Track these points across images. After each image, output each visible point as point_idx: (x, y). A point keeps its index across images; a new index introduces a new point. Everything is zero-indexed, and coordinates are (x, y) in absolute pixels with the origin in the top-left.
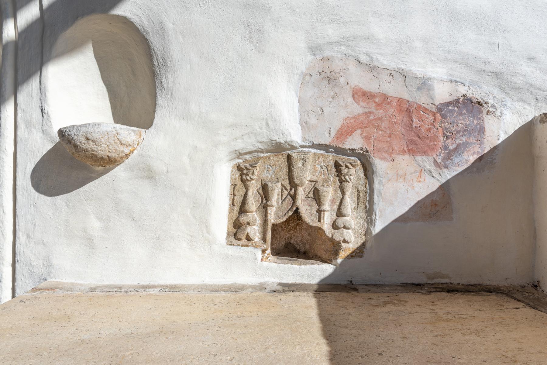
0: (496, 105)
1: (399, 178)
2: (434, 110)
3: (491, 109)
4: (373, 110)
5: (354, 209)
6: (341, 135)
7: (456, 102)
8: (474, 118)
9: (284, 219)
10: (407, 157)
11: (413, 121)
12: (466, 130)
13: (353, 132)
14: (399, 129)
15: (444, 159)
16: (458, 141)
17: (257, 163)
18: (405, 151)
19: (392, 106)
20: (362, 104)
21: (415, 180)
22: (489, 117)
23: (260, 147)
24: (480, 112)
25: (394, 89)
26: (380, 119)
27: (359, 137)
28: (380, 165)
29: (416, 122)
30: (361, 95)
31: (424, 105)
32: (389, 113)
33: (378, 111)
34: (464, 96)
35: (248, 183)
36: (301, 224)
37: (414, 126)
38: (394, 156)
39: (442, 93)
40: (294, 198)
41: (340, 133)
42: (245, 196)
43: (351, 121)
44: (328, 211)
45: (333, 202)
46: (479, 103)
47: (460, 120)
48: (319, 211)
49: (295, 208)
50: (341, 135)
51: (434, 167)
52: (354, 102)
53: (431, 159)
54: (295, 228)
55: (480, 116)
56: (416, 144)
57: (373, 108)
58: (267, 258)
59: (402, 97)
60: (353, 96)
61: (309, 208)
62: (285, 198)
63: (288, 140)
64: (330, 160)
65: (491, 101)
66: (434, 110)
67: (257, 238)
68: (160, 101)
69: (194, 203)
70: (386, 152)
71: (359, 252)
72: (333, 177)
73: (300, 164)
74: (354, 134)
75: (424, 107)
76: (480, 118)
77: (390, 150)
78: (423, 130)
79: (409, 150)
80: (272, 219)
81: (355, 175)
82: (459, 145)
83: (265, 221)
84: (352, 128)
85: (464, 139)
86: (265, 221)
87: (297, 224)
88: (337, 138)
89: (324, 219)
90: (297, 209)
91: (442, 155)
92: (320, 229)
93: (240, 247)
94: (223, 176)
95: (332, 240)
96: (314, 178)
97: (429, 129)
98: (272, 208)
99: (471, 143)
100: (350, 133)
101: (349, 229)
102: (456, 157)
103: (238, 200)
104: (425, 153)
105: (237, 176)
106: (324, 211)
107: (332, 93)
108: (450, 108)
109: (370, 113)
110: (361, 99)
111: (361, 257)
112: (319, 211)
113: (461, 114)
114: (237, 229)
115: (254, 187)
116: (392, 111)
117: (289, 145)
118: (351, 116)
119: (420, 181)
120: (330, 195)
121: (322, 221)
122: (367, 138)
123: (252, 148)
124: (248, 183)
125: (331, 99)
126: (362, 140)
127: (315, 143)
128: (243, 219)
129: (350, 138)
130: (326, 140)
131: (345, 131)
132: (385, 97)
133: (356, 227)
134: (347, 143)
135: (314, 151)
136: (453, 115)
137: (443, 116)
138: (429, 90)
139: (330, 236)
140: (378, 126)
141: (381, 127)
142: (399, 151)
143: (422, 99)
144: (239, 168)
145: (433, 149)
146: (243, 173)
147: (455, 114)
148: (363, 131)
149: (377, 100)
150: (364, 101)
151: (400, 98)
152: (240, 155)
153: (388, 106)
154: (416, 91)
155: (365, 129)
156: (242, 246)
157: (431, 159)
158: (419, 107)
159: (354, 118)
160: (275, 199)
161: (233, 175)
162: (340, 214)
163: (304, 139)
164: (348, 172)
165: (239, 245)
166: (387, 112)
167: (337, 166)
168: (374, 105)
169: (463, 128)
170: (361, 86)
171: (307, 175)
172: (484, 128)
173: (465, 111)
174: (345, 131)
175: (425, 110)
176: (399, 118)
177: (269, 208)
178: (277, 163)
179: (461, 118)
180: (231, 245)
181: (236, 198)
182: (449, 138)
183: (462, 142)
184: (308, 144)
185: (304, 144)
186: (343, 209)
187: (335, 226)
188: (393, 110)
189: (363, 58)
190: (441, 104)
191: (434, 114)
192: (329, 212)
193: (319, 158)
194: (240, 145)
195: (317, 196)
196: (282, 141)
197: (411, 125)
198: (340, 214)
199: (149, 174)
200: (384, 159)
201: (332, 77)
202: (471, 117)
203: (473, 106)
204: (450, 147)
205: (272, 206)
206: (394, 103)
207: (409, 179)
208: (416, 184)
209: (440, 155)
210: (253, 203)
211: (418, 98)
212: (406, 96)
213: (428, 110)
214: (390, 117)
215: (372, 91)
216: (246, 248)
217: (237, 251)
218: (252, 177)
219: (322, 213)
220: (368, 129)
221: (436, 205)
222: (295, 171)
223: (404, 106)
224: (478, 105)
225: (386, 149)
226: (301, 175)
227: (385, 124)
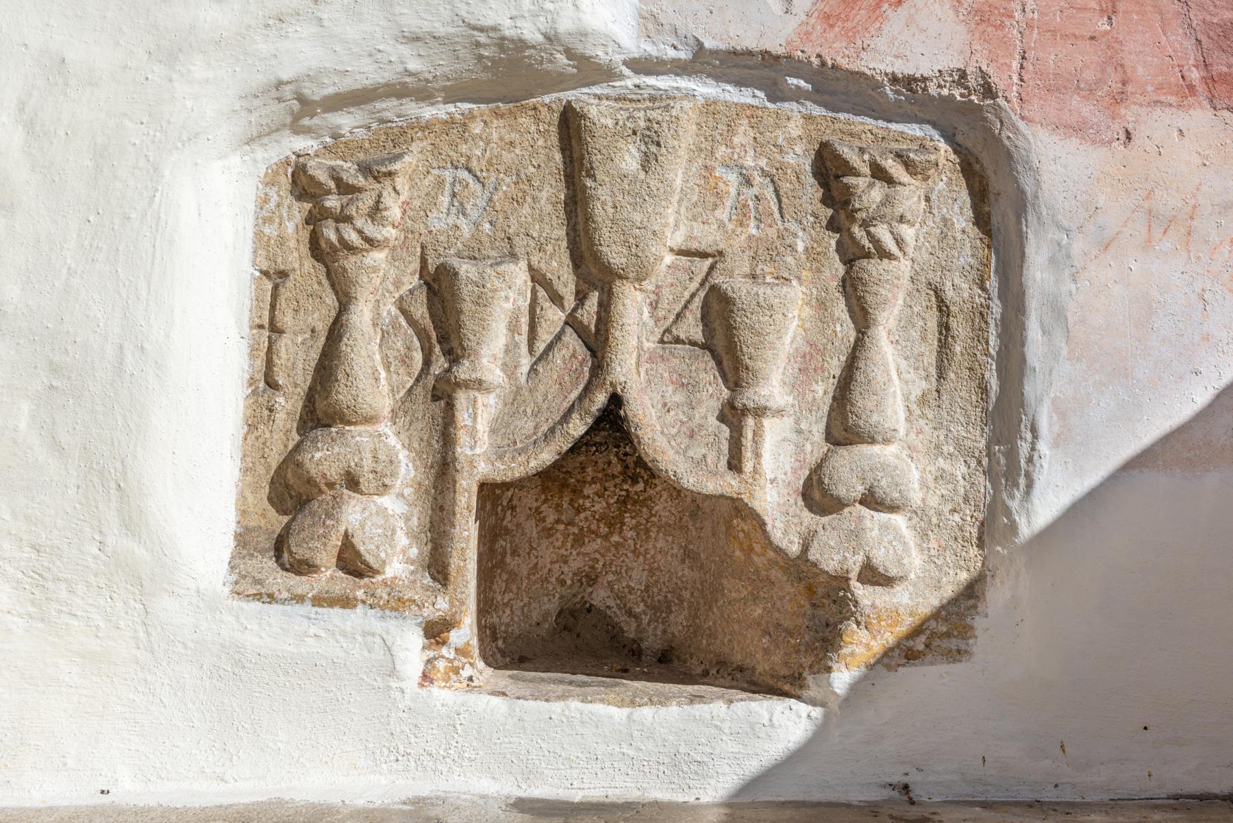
1: (1157, 233)
5: (923, 400)
9: (547, 456)
17: (398, 157)
18: (1191, 87)
23: (413, 65)
28: (1057, 163)
35: (350, 263)
36: (647, 502)
38: (1129, 114)
40: (597, 342)
42: (336, 331)
44: (780, 412)
45: (807, 365)
48: (733, 415)
49: (601, 399)
54: (615, 523)
58: (456, 671)
61: (679, 398)
62: (550, 347)
63: (565, 25)
64: (791, 141)
67: (398, 560)
69: (54, 369)
71: (943, 633)
72: (806, 234)
73: (630, 160)
79: (1210, 80)
80: (481, 454)
81: (923, 218)
83: (443, 469)
86: (443, 469)
87: (623, 502)
88: (828, 19)
89: (758, 455)
90: (616, 400)
92: (739, 510)
93: (307, 608)
94: (214, 225)
95: (801, 569)
96: (708, 237)
98: (481, 399)
101: (893, 508)
103: (297, 358)
106: (760, 412)
111: (957, 655)
112: (733, 415)
114: (292, 515)
115: (383, 286)
117: (569, 53)
120: (789, 324)
121: (748, 466)
123: (368, 74)
124: (350, 263)
126: (962, 28)
127: (709, 44)
129: (895, 21)
133: (933, 501)
134: (880, 43)
135: (705, 89)
139: (795, 549)
142: (1159, 88)
144: (303, 185)
146: (320, 212)
152: (303, 108)
156: (318, 601)
160: (494, 350)
162: (844, 427)
163: (650, 22)
164: (887, 201)
165: (300, 599)
167: (829, 170)
171: (668, 220)
177: (461, 398)
178: (507, 157)
180: (258, 597)
181: (285, 346)
184: (672, 53)
185: (651, 50)
186: (862, 401)
192: (788, 422)
194: (304, 55)
195: (720, 333)
196: (531, 32)
198: (844, 427)
200: (1078, 129)
205: (479, 385)
216: (337, 610)
218: (371, 230)
219: (750, 422)
222: (604, 199)
225: (1089, 75)
226: (637, 217)
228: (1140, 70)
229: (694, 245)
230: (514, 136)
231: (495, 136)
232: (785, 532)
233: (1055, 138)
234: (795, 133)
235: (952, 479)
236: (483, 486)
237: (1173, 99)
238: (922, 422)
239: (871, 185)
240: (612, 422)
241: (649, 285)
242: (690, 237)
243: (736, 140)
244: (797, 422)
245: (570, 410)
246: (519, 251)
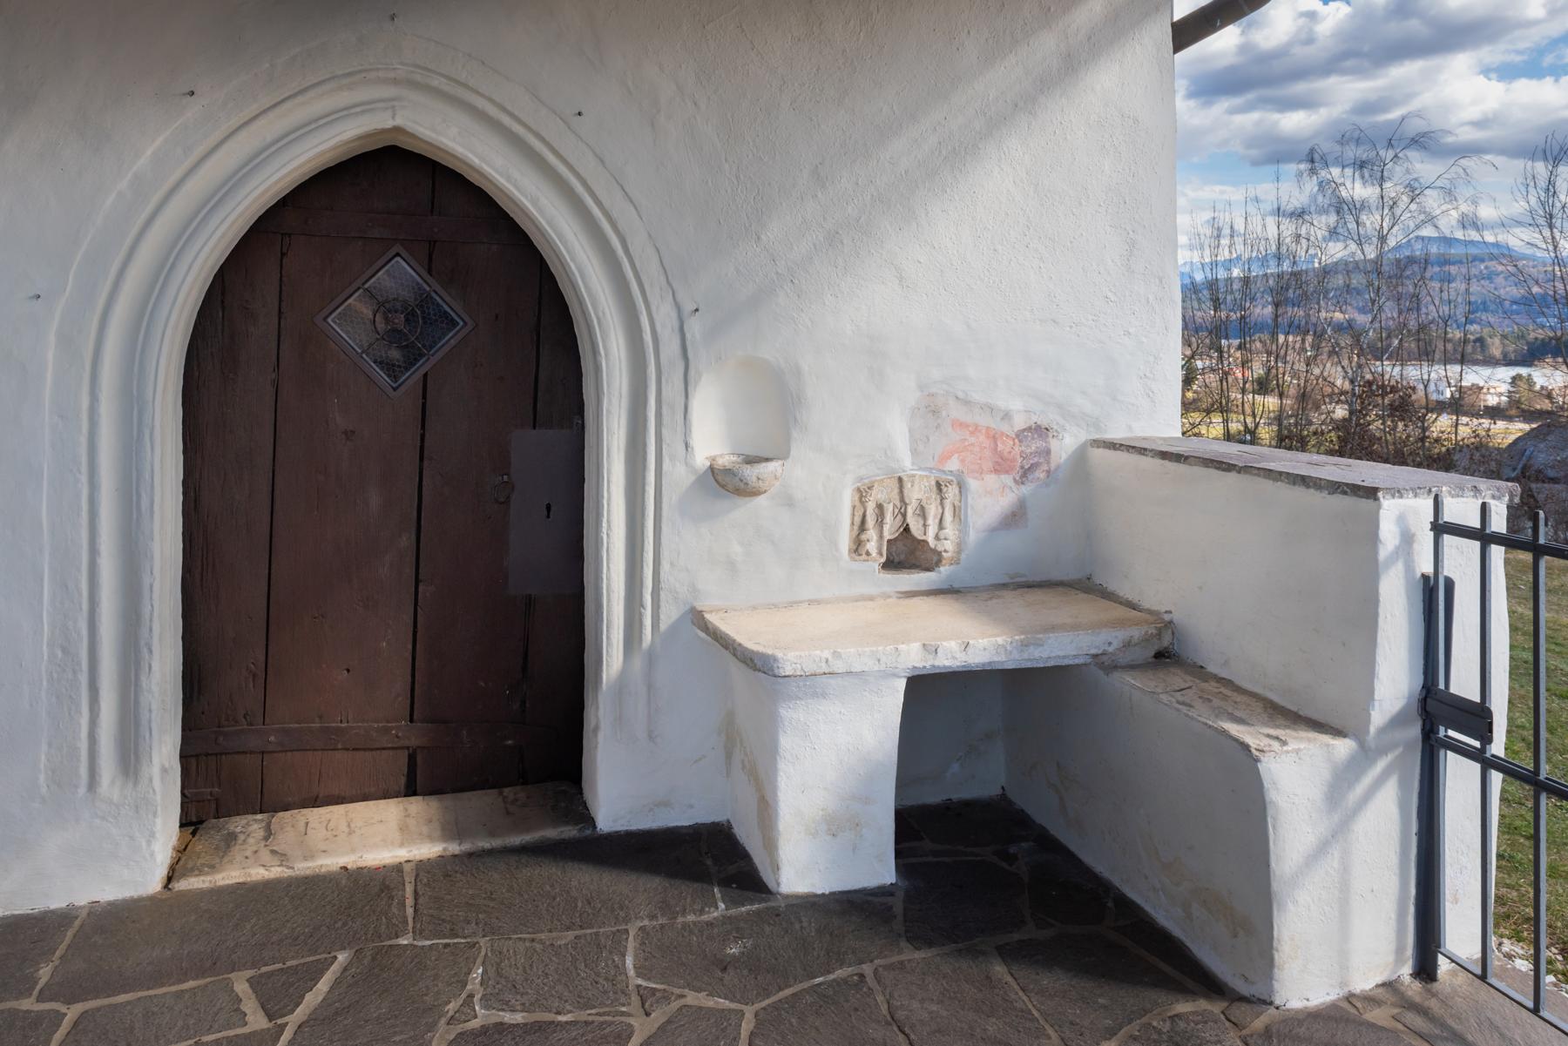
7: (1029, 429)
10: (993, 476)
14: (988, 453)
25: (984, 420)
28: (973, 484)
29: (1000, 447)
39: (1020, 422)
40: (904, 516)
42: (864, 516)
48: (925, 525)
67: (874, 553)
68: (795, 434)
71: (956, 561)
72: (934, 495)
80: (887, 536)
81: (951, 492)
83: (881, 537)
86: (881, 537)
92: (925, 541)
94: (847, 498)
103: (858, 520)
104: (1007, 472)
112: (925, 525)
114: (858, 546)
115: (871, 506)
116: (982, 438)
120: (933, 511)
122: (963, 461)
128: (863, 537)
130: (931, 464)
143: (1005, 428)
144: (859, 490)
146: (862, 494)
160: (889, 518)
162: (941, 526)
167: (938, 485)
171: (914, 494)
187: (937, 538)
189: (961, 395)
195: (922, 513)
198: (941, 526)
199: (789, 502)
210: (871, 522)
212: (993, 425)
217: (859, 566)
222: (906, 492)
227: (977, 449)
240: (907, 529)
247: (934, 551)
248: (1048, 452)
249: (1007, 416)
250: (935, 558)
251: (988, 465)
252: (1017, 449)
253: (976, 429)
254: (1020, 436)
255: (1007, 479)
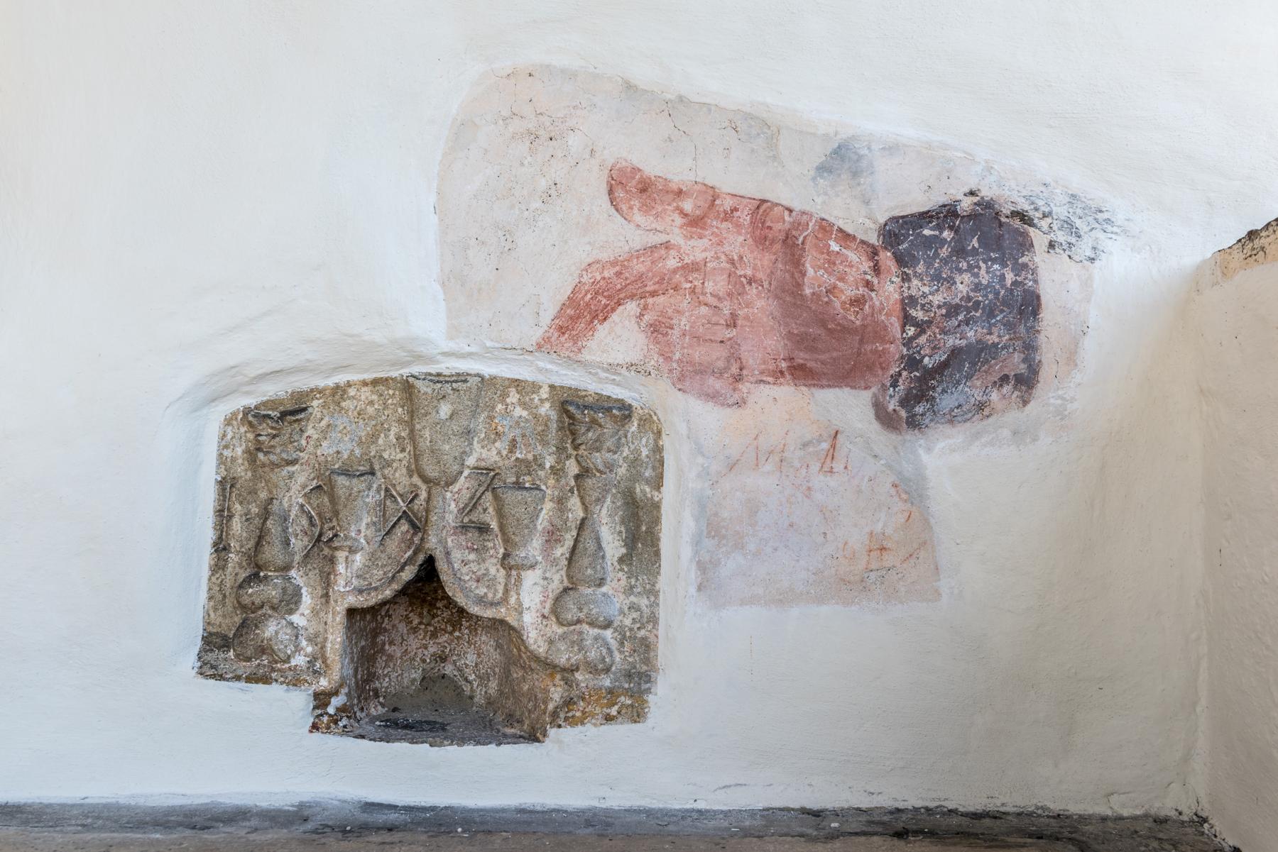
0: (1078, 223)
2: (873, 239)
3: (1061, 237)
4: (677, 238)
5: (621, 560)
6: (574, 319)
7: (947, 214)
8: (1004, 265)
11: (804, 274)
12: (977, 303)
13: (613, 310)
14: (760, 305)
15: (905, 402)
16: (952, 341)
17: (304, 409)
18: (782, 372)
19: (738, 226)
20: (638, 217)
21: (815, 467)
22: (1052, 257)
24: (1026, 245)
25: (737, 177)
26: (694, 267)
27: (632, 324)
29: (814, 276)
30: (631, 188)
31: (841, 224)
32: (727, 248)
33: (693, 242)
34: (972, 193)
37: (808, 291)
38: (744, 387)
41: (570, 312)
43: (606, 274)
44: (532, 567)
45: (553, 537)
46: (1022, 216)
47: (960, 271)
50: (574, 319)
51: (876, 426)
52: (613, 210)
53: (866, 397)
55: (1024, 260)
56: (812, 349)
57: (677, 231)
59: (767, 196)
60: (611, 192)
61: (472, 556)
64: (542, 401)
65: (1061, 211)
66: (873, 239)
70: (720, 374)
74: (615, 317)
75: (840, 230)
76: (1025, 266)
77: (734, 369)
78: (837, 304)
82: (955, 352)
84: (609, 297)
85: (970, 334)
88: (562, 330)
90: (430, 561)
91: (901, 388)
97: (858, 302)
99: (995, 345)
100: (601, 315)
102: (944, 391)
105: (239, 451)
106: (521, 567)
107: (543, 184)
108: (927, 232)
109: (667, 246)
110: (636, 203)
113: (960, 251)
116: (737, 242)
118: (605, 256)
119: (831, 471)
121: (513, 600)
122: (658, 330)
125: (538, 204)
126: (643, 336)
129: (602, 330)
131: (582, 313)
132: (713, 195)
133: (628, 622)
136: (936, 255)
137: (900, 260)
138: (855, 174)
140: (693, 291)
141: (704, 294)
142: (762, 373)
145: (870, 368)
147: (944, 252)
148: (645, 308)
149: (688, 206)
150: (646, 209)
151: (763, 201)
153: (725, 225)
154: (814, 179)
155: (650, 301)
157: (866, 397)
158: (825, 227)
159: (614, 263)
161: (226, 447)
166: (720, 243)
168: (679, 220)
169: (969, 299)
170: (636, 160)
172: (1038, 297)
173: (975, 242)
174: (588, 305)
175: (846, 237)
176: (760, 263)
178: (370, 410)
179: (964, 265)
182: (923, 332)
183: (964, 342)
184: (468, 349)
188: (741, 239)
190: (895, 219)
191: (873, 253)
193: (504, 395)
197: (799, 286)
200: (713, 397)
201: (541, 132)
202: (994, 261)
203: (1001, 225)
204: (926, 360)
206: (744, 217)
207: (797, 464)
208: (819, 481)
209: (894, 385)
211: (819, 200)
213: (854, 238)
214: (732, 262)
215: (669, 177)
220: (661, 299)
221: (883, 549)
223: (779, 226)
224: (1017, 223)
225: (720, 364)
227: (716, 285)
228: (751, 361)
229: (483, 464)
230: (375, 397)
231: (363, 398)
232: (535, 642)
233: (699, 402)
234: (545, 396)
235: (639, 609)
236: (351, 612)
237: (770, 379)
238: (621, 574)
239: (588, 430)
241: (456, 487)
242: (479, 460)
243: (508, 400)
244: (545, 572)
245: (406, 564)
246: (377, 467)
247: (551, 667)
248: (1028, 305)
249: (842, 160)
250: (557, 694)
251: (764, 341)
252: (890, 290)
253: (706, 211)
254: (904, 237)
255: (850, 407)
